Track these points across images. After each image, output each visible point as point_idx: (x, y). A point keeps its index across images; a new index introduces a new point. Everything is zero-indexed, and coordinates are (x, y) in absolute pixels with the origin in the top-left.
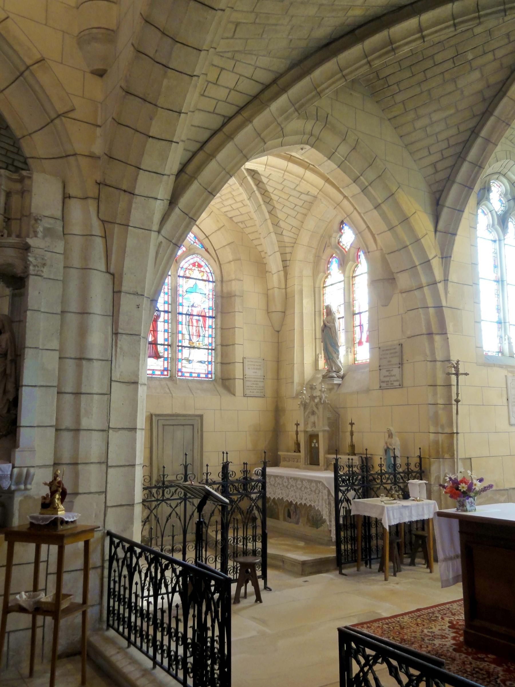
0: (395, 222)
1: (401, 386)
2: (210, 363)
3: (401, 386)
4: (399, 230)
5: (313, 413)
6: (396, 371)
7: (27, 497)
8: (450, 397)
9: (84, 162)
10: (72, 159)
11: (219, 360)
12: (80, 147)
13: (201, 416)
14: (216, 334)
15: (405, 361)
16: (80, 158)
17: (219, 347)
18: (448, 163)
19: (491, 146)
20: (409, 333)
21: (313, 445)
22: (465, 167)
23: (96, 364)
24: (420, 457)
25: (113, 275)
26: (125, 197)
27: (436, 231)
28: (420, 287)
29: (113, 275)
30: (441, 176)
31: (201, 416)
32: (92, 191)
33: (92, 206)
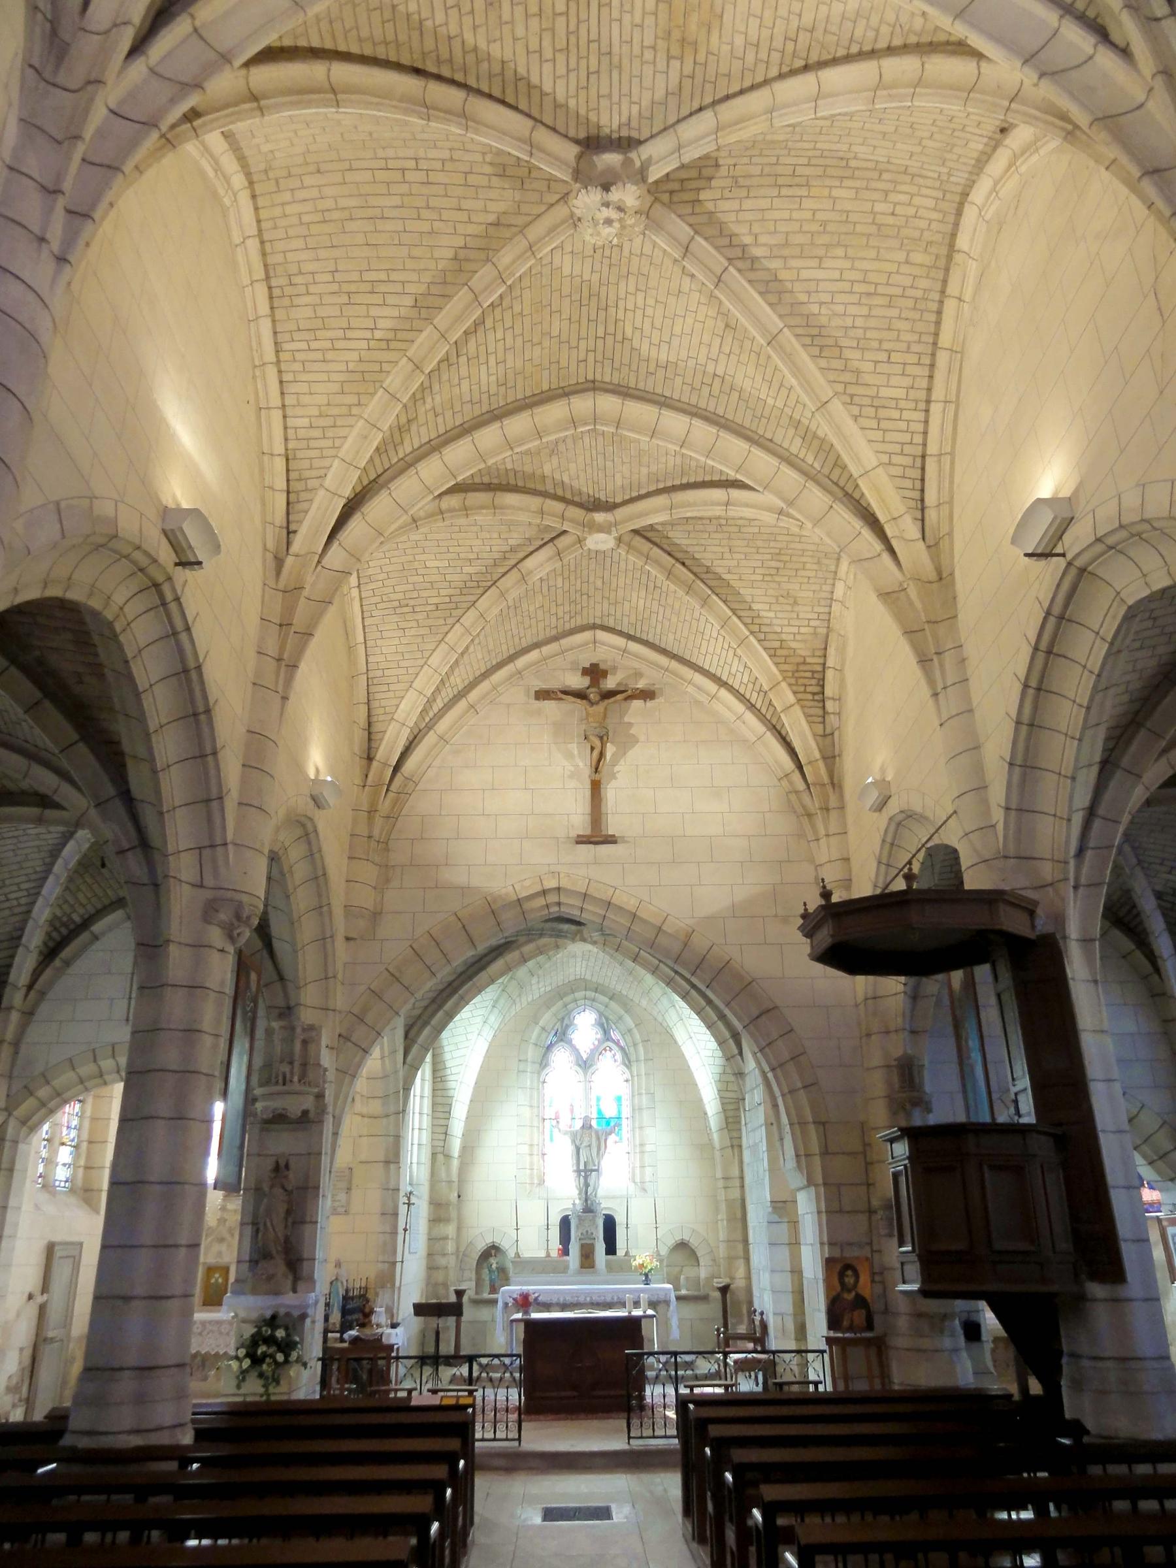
0: (386, 1054)
1: (346, 1212)
3: (346, 1212)
4: (387, 1061)
5: (221, 1240)
6: (342, 1196)
8: (395, 1227)
13: (81, 1244)
15: (354, 1187)
17: (84, 1145)
18: (425, 1003)
19: (463, 1003)
20: (363, 1157)
21: (213, 1281)
22: (440, 1014)
24: (366, 1289)
26: (361, 1053)
27: (404, 1063)
28: (387, 1116)
30: (417, 1012)
31: (81, 1244)
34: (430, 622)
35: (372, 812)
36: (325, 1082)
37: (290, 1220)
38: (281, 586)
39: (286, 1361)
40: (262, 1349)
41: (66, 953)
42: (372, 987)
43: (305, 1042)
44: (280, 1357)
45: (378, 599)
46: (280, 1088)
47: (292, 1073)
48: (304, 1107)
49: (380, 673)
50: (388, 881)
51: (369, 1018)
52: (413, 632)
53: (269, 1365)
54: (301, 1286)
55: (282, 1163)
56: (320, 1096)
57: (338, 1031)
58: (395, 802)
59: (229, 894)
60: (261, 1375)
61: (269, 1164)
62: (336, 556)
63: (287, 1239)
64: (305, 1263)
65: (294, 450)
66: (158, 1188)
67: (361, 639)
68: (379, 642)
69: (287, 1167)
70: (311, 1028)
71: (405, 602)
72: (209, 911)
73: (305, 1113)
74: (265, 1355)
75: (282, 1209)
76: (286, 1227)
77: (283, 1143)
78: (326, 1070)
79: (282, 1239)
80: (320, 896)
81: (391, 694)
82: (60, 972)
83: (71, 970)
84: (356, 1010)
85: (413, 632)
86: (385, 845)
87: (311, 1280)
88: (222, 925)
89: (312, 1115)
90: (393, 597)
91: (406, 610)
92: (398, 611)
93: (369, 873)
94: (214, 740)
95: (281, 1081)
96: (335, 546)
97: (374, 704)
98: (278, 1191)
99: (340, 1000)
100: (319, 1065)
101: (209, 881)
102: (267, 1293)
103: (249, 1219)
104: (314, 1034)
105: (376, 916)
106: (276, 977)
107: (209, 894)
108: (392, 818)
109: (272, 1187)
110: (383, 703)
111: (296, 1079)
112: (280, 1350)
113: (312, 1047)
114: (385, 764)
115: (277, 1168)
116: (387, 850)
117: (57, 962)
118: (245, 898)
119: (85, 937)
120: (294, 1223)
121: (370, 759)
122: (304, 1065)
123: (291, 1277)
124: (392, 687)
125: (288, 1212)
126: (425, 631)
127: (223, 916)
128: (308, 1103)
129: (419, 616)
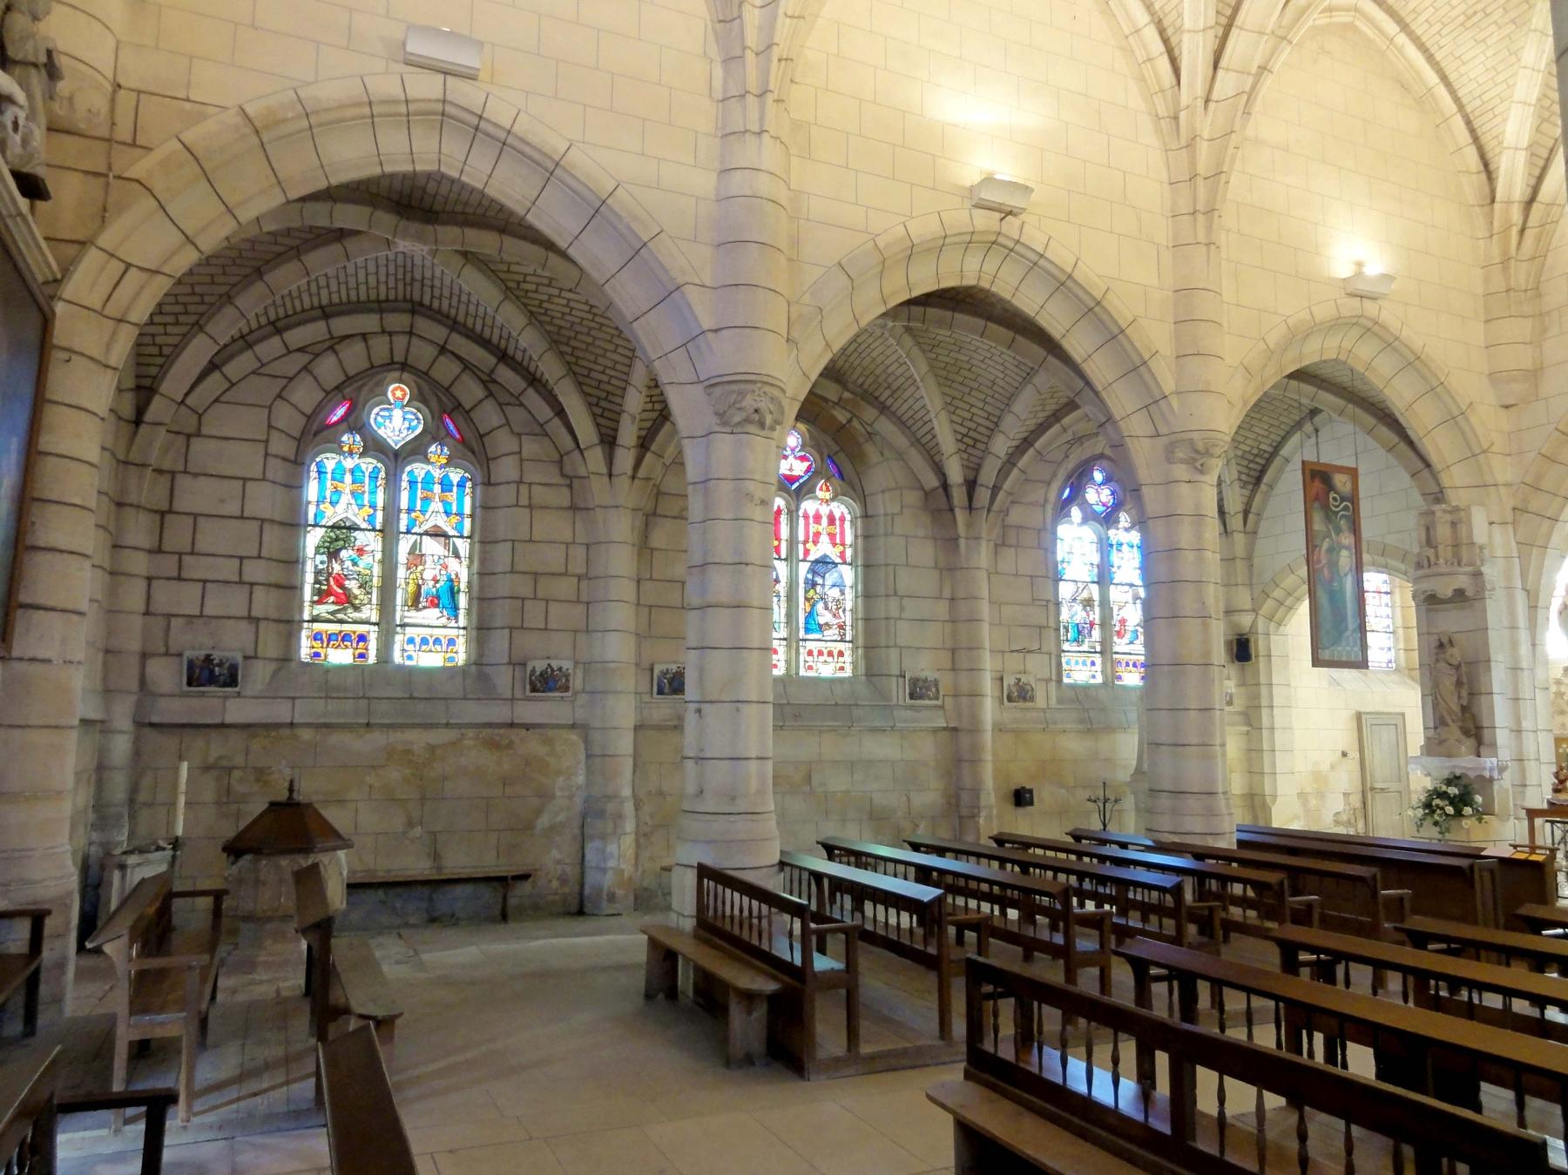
2: (1389, 649)
7: (1501, 786)
9: (1503, 490)
10: (1492, 489)
11: (1401, 645)
12: (1500, 479)
13: (1403, 715)
14: (1393, 612)
16: (1501, 488)
17: (1400, 631)
23: (1526, 672)
25: (1528, 591)
26: (1547, 523)
29: (1528, 591)
32: (1509, 517)
33: (1510, 529)
34: (1512, 15)
35: (1505, 262)
36: (1482, 560)
37: (1464, 693)
38: (1183, 143)
39: (1459, 814)
40: (1437, 802)
41: (1266, 479)
42: (1543, 451)
43: (1454, 524)
44: (1450, 810)
45: (1437, 27)
46: (1426, 571)
47: (1437, 557)
48: (1457, 586)
49: (1478, 102)
50: (1544, 330)
51: (1546, 484)
52: (1495, 38)
53: (1440, 815)
54: (1483, 750)
55: (1445, 640)
56: (1477, 575)
57: (1512, 503)
58: (1538, 239)
59: (1179, 436)
60: (1436, 824)
61: (1434, 641)
62: (1226, 84)
63: (1464, 709)
64: (1486, 731)
65: (1162, 8)
66: (1166, 668)
67: (1432, 78)
68: (1463, 69)
69: (1451, 642)
70: (1457, 509)
71: (1470, 12)
72: (1169, 455)
73: (1460, 594)
74: (1437, 806)
75: (1448, 682)
76: (1459, 697)
77: (1452, 621)
78: (1481, 548)
79: (1457, 709)
80: (1424, 378)
81: (1499, 119)
82: (1267, 496)
83: (1274, 492)
84: (1529, 480)
85: (1495, 38)
86: (1537, 292)
87: (1493, 745)
88: (1183, 461)
89: (1470, 593)
90: (1454, 13)
91: (1475, 19)
92: (1468, 24)
93: (1522, 329)
94: (1116, 322)
95: (1426, 563)
96: (1220, 73)
97: (1484, 139)
98: (1442, 665)
99: (1503, 471)
100: (1473, 544)
101: (1163, 430)
102: (1441, 755)
103: (1428, 692)
104: (1462, 513)
105: (1535, 374)
106: (1420, 465)
107: (1165, 440)
108: (1539, 257)
109: (1437, 660)
110: (1494, 132)
111: (1441, 561)
112: (1452, 803)
113: (1463, 529)
114: (1509, 203)
115: (1441, 646)
116: (1540, 296)
117: (1263, 487)
118: (1195, 435)
119: (1277, 462)
120: (1471, 694)
121: (1493, 201)
122: (1456, 546)
123: (1471, 742)
124: (1497, 111)
125: (1459, 684)
126: (1510, 28)
127: (1180, 454)
128: (1462, 581)
129: (1495, 17)
